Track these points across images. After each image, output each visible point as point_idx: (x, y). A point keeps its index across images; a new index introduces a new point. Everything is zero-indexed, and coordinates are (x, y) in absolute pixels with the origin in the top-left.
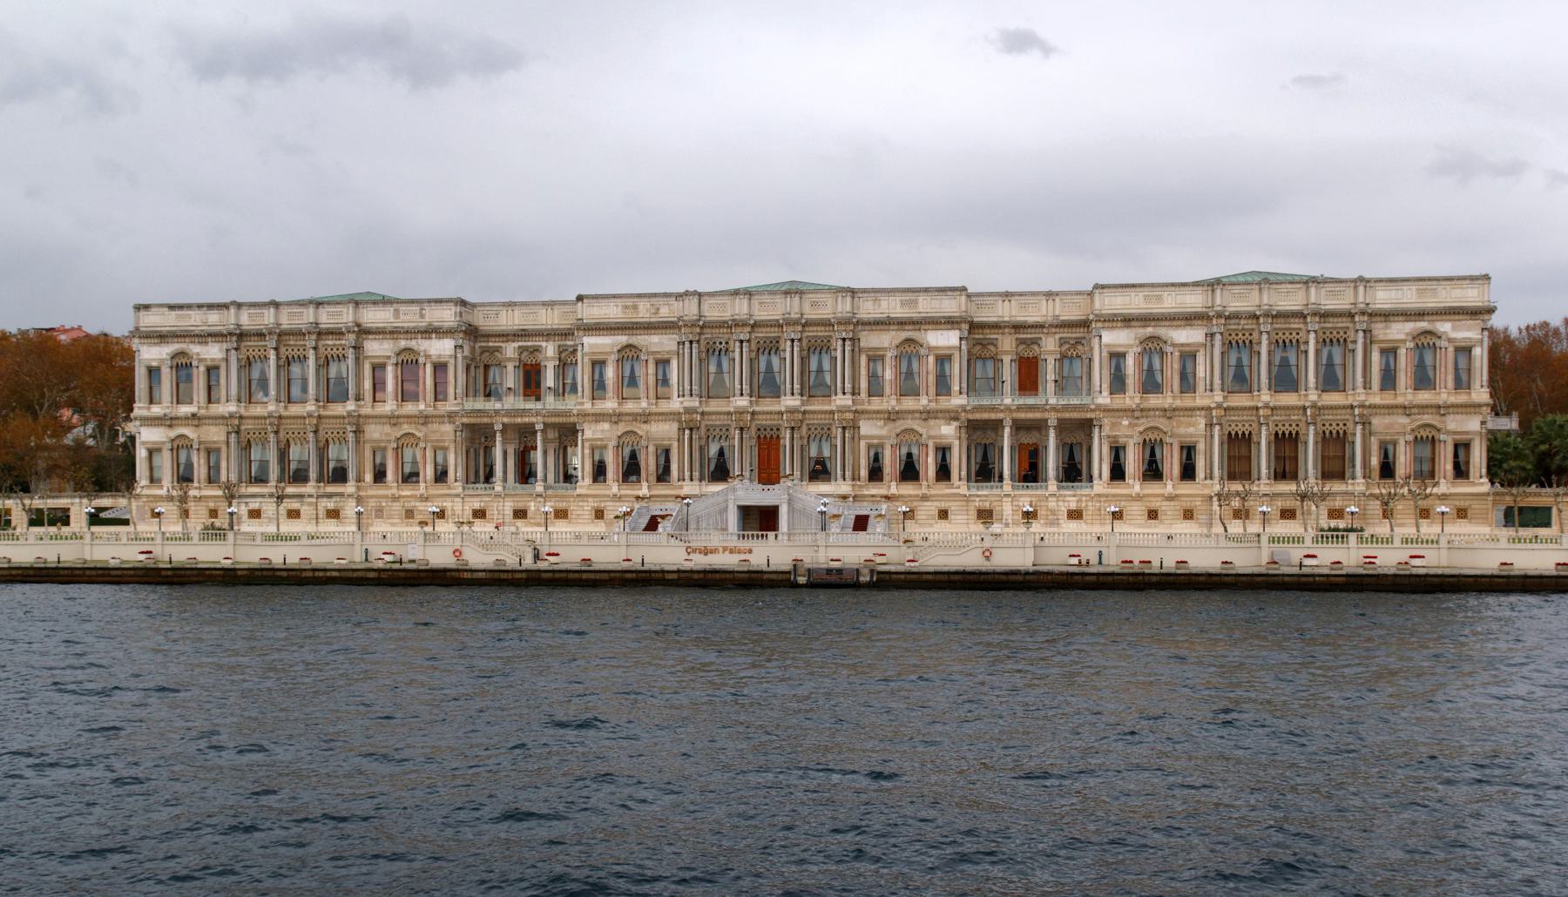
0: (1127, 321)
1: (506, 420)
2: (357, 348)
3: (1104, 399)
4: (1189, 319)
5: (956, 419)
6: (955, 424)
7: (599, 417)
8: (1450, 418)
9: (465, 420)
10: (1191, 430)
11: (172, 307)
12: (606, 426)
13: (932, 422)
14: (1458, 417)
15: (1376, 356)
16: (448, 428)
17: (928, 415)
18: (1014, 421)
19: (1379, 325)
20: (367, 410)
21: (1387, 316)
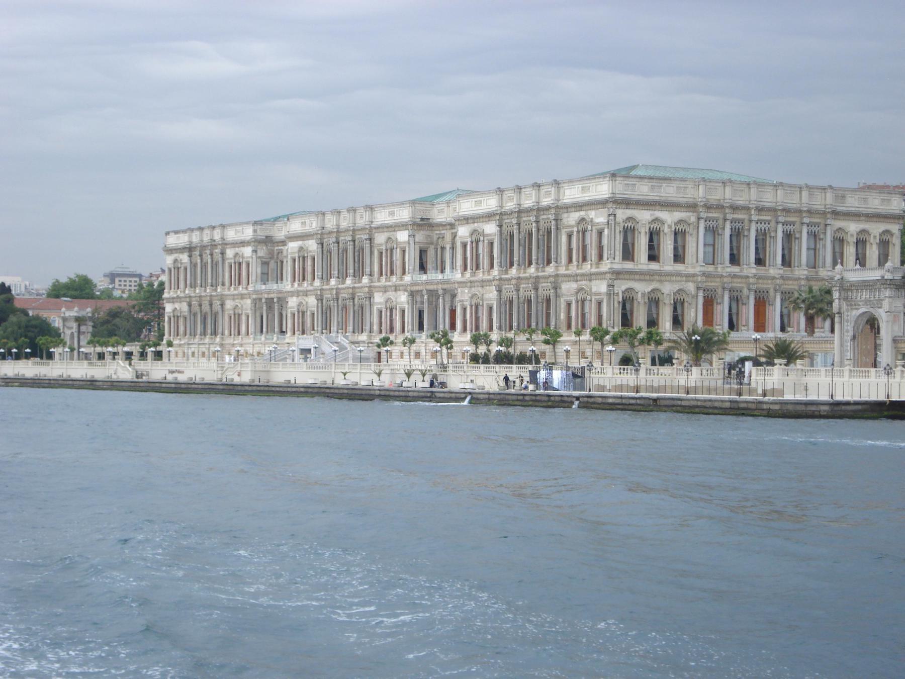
0: (467, 220)
1: (266, 296)
2: (223, 253)
3: (458, 276)
4: (489, 217)
5: (406, 290)
6: (406, 294)
7: (292, 294)
8: (594, 282)
9: (254, 296)
10: (491, 295)
11: (176, 232)
12: (295, 299)
13: (399, 293)
14: (597, 282)
15: (564, 239)
16: (249, 301)
17: (396, 288)
18: (427, 291)
19: (565, 215)
20: (226, 292)
21: (569, 208)
